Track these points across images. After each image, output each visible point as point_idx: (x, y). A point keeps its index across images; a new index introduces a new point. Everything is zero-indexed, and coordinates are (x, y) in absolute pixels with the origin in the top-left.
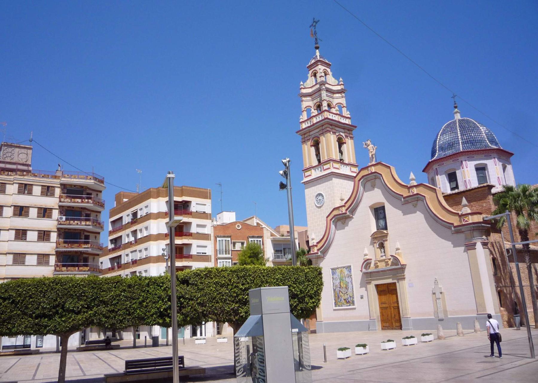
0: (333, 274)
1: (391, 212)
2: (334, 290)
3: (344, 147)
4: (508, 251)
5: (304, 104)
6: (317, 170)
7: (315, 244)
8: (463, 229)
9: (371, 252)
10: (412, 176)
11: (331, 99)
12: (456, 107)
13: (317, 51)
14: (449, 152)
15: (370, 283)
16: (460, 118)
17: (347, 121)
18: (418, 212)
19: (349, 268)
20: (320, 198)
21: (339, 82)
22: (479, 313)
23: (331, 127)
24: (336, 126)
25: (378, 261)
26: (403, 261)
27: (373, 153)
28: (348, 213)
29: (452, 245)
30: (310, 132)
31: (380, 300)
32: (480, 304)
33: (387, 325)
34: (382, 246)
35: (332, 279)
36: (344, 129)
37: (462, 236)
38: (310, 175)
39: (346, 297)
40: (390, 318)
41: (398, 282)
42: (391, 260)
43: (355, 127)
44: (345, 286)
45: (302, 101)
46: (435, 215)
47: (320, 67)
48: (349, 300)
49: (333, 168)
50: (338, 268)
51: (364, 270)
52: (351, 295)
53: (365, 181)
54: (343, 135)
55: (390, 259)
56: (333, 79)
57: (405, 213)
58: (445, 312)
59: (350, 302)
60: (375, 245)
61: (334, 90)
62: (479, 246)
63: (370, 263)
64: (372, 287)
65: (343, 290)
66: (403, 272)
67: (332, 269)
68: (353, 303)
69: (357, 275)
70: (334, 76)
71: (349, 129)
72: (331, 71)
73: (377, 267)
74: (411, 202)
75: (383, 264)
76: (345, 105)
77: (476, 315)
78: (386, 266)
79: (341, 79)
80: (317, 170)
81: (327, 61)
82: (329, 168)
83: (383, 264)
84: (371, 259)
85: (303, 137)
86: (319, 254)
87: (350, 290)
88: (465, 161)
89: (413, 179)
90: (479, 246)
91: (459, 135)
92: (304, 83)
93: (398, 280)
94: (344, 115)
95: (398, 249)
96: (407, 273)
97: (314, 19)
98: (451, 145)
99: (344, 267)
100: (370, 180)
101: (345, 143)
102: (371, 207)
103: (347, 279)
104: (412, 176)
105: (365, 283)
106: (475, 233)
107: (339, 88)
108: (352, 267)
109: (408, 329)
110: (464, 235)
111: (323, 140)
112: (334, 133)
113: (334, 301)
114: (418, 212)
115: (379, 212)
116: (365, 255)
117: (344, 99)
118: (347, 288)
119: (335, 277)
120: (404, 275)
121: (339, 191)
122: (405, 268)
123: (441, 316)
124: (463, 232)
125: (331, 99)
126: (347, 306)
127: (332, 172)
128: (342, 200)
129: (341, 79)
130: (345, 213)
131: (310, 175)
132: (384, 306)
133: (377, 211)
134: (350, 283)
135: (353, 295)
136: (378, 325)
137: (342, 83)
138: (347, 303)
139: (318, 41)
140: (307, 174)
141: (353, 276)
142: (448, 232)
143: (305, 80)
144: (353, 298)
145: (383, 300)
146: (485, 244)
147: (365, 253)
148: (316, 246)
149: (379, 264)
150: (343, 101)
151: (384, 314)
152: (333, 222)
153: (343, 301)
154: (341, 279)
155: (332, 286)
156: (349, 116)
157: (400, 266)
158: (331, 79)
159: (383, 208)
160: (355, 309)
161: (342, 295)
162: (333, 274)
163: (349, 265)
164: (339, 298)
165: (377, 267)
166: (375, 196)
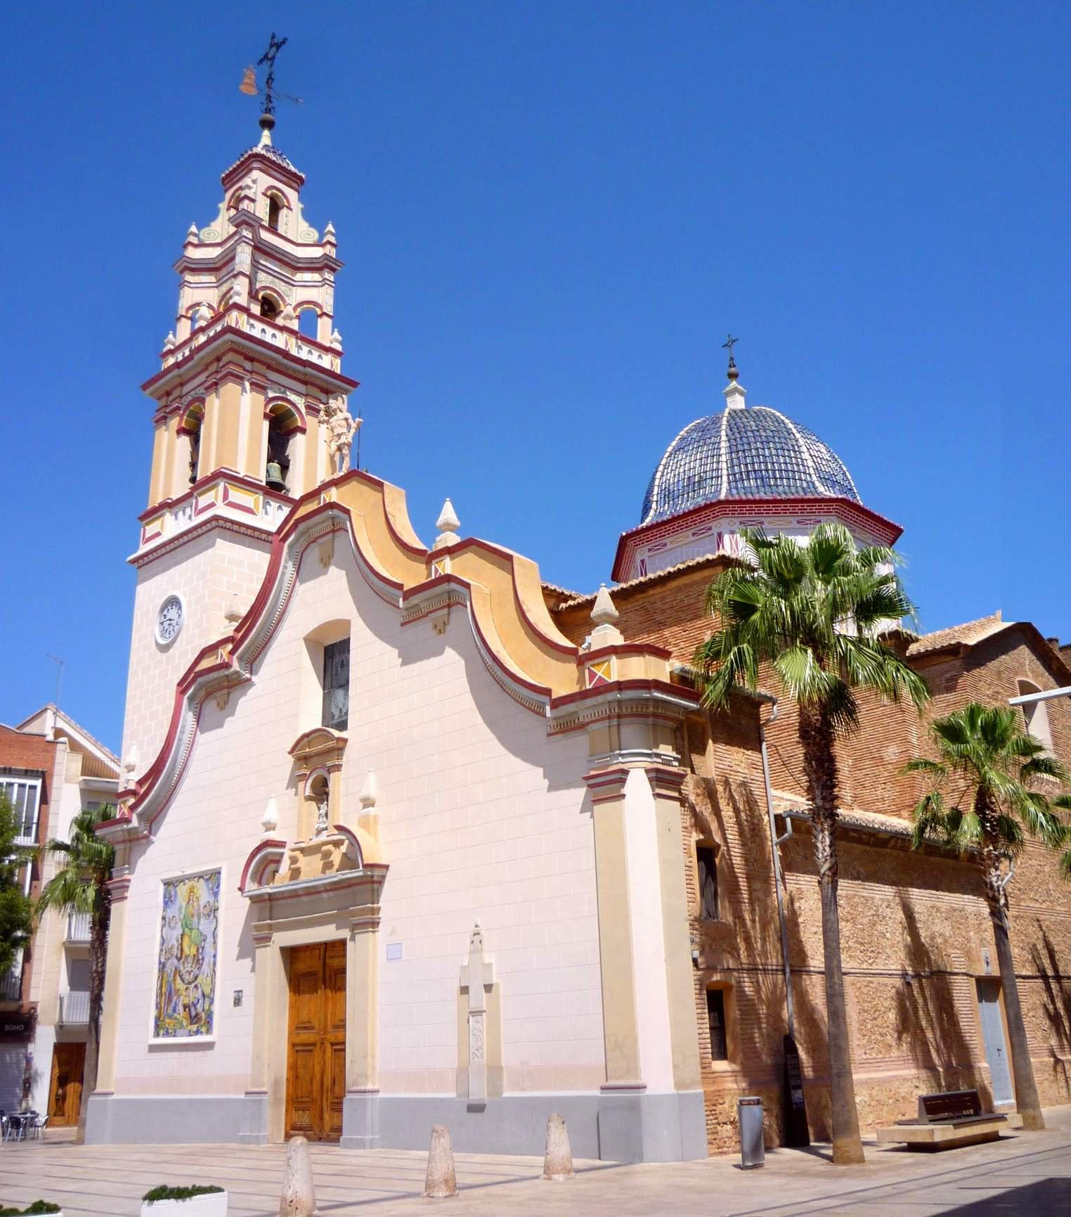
0: (166, 903)
1: (370, 655)
2: (162, 966)
3: (297, 447)
4: (779, 820)
5: (188, 297)
6: (180, 514)
7: (132, 786)
8: (583, 710)
9: (285, 815)
10: (448, 513)
11: (281, 287)
12: (733, 376)
14: (686, 505)
15: (268, 939)
17: (326, 361)
18: (449, 652)
20: (172, 613)
21: (322, 234)
22: (612, 1083)
23: (248, 365)
24: (269, 367)
25: (302, 850)
26: (373, 851)
27: (343, 440)
28: (236, 666)
29: (546, 782)
30: (182, 385)
31: (294, 1008)
32: (620, 1044)
33: (305, 1119)
34: (321, 793)
35: (159, 922)
36: (306, 383)
37: (579, 743)
38: (158, 534)
40: (316, 1095)
41: (353, 939)
42: (343, 848)
43: (354, 384)
44: (193, 951)
45: (182, 284)
46: (495, 659)
47: (256, 174)
49: (215, 502)
50: (181, 880)
51: (251, 887)
52: (207, 991)
53: (303, 543)
54: (300, 402)
55: (337, 844)
56: (304, 225)
57: (408, 658)
58: (495, 1070)
59: (200, 1019)
60: (301, 785)
61: (298, 259)
62: (638, 784)
63: (277, 861)
64: (270, 958)
65: (186, 968)
66: (375, 896)
67: (168, 884)
69: (233, 910)
70: (308, 215)
71: (323, 386)
72: (300, 199)
73: (295, 873)
74: (427, 609)
75: (316, 862)
76: (329, 309)
77: (597, 1093)
78: (323, 872)
79: (330, 228)
80: (180, 514)
81: (292, 168)
82: (212, 505)
83: (316, 862)
84: (281, 844)
85: (163, 402)
86: (135, 822)
87: (206, 968)
88: (732, 533)
89: (449, 527)
90: (638, 784)
91: (723, 451)
92: (199, 229)
93: (356, 927)
94: (319, 340)
95: (368, 803)
96: (389, 902)
98: (695, 484)
99: (200, 876)
100: (314, 532)
101: (303, 431)
102: (310, 641)
104: (448, 513)
105: (254, 940)
106: (630, 731)
107: (317, 252)
109: (360, 1144)
110: (575, 732)
111: (214, 406)
112: (258, 387)
113: (153, 1013)
114: (449, 652)
115: (333, 659)
116: (269, 827)
117: (331, 291)
118: (198, 961)
120: (375, 911)
121: (221, 581)
122: (381, 882)
123: (479, 1093)
124: (582, 726)
125: (281, 287)
127: (216, 518)
128: (231, 618)
129: (330, 228)
130: (226, 666)
131: (158, 534)
132: (306, 1037)
133: (332, 657)
134: (210, 940)
135: (213, 990)
136: (274, 1117)
137: (333, 240)
139: (275, 103)
140: (151, 529)
141: (221, 914)
142: (535, 729)
143: (206, 219)
145: (304, 1016)
146: (663, 781)
147: (265, 818)
149: (303, 862)
150: (325, 297)
151: (301, 1071)
152: (191, 699)
153: (181, 1014)
156: (339, 347)
157: (359, 873)
158: (294, 223)
159: (344, 646)
160: (209, 1046)
162: (168, 901)
164: (170, 1000)
165: (295, 873)
166: (323, 599)
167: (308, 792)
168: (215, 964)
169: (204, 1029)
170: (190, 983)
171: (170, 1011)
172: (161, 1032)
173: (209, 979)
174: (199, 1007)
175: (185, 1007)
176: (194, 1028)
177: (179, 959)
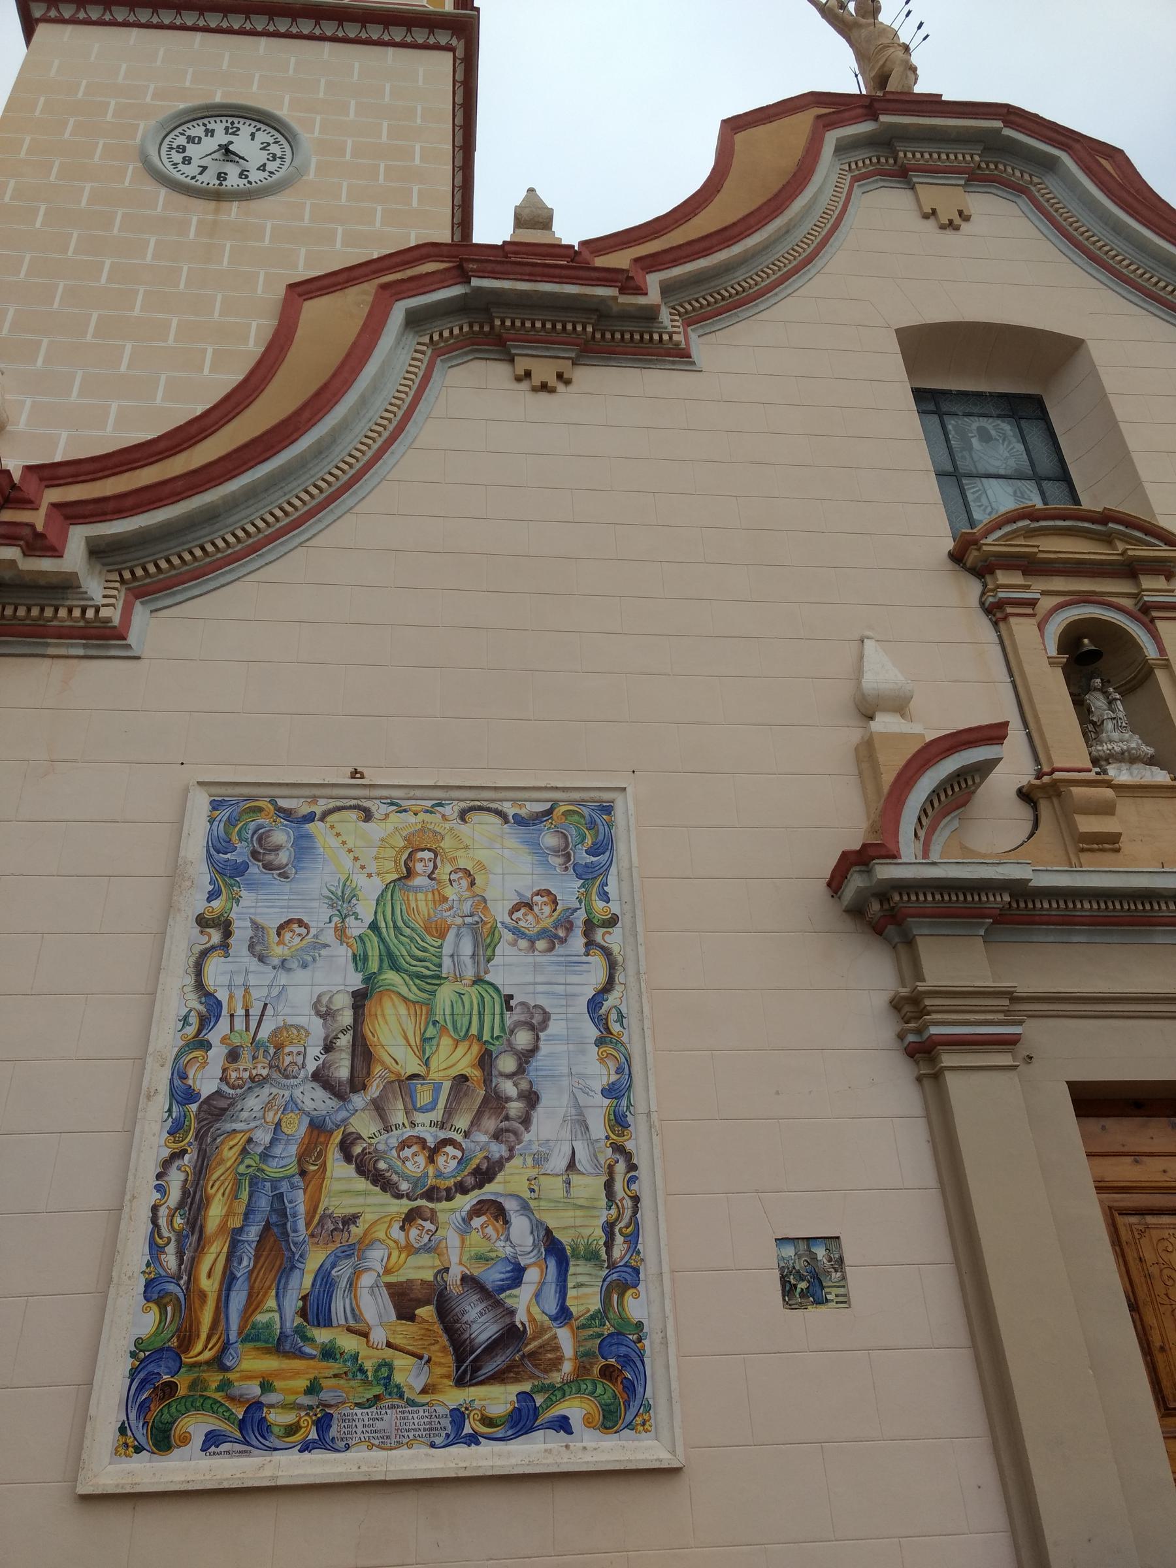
0: (227, 874)
2: (200, 1121)
19: (582, 831)
35: (184, 938)
39: (458, 1245)
48: (524, 1302)
52: (580, 1226)
68: (618, 1376)
103: (513, 969)
118: (497, 1092)
126: (458, 1429)
130: (627, 283)
134: (570, 1028)
135: (625, 1227)
138: (469, 1366)
144: (624, 1279)
154: (389, 961)
155: (167, 1039)
167: (1053, 651)
168: (619, 1122)
169: (574, 1409)
170: (431, 1194)
171: (279, 1312)
172: (196, 1426)
173: (589, 1186)
174: (524, 1302)
175: (404, 1301)
176: (498, 1399)
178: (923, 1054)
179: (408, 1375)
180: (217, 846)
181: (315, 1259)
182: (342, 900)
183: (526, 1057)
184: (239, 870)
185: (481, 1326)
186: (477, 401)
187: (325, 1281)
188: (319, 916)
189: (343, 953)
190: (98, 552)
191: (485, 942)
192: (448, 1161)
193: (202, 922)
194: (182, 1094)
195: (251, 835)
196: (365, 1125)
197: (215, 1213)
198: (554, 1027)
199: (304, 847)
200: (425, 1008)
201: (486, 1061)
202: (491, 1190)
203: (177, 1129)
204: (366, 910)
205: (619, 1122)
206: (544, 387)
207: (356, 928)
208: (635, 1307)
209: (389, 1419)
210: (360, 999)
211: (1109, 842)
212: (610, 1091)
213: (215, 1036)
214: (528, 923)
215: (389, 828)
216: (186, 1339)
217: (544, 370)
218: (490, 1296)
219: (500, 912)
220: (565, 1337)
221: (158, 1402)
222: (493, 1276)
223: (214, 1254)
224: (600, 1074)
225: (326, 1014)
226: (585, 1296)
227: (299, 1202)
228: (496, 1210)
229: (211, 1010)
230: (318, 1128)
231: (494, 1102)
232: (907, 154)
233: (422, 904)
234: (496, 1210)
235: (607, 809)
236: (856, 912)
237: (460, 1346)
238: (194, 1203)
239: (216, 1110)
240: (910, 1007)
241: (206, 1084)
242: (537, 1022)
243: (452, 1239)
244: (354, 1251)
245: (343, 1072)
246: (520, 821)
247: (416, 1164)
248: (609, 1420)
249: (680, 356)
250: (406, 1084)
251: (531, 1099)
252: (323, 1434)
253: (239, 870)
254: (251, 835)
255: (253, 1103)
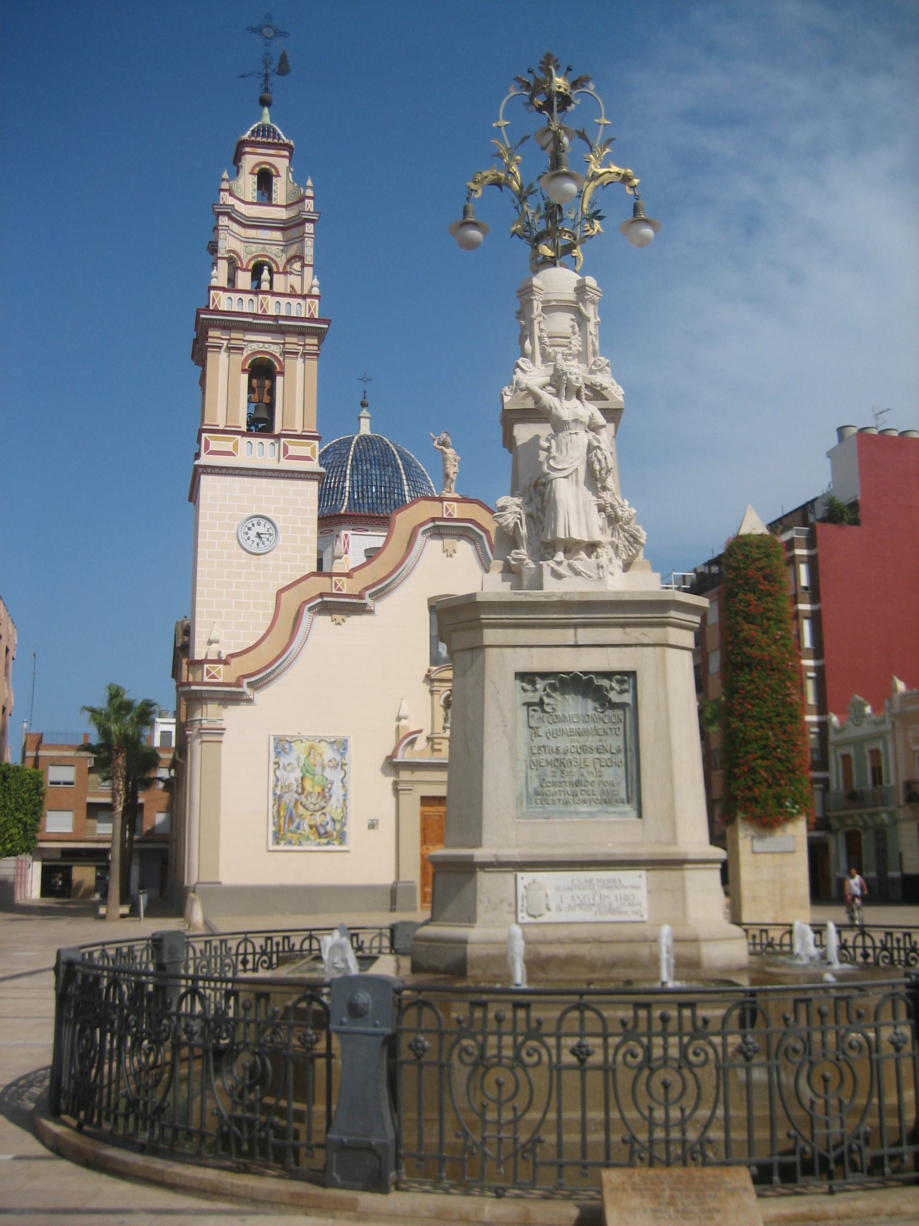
0: (278, 754)
2: (278, 799)
13: (266, 110)
16: (369, 433)
19: (341, 745)
35: (272, 767)
39: (318, 819)
44: (318, 789)
48: (329, 828)
52: (338, 817)
59: (331, 834)
65: (310, 801)
68: (342, 837)
82: (308, 459)
97: (268, 17)
102: (430, 600)
103: (328, 773)
108: (351, 745)
113: (272, 828)
118: (325, 795)
119: (283, 760)
126: (319, 844)
135: (345, 817)
138: (320, 836)
141: (352, 769)
144: (344, 825)
148: (226, 663)
154: (307, 772)
155: (271, 785)
161: (306, 813)
163: (342, 734)
164: (291, 820)
167: (442, 703)
168: (345, 800)
169: (336, 842)
171: (293, 827)
172: (283, 842)
173: (339, 810)
175: (311, 827)
176: (325, 841)
177: (300, 794)
178: (396, 792)
179: (312, 837)
180: (276, 748)
181: (297, 821)
182: (298, 759)
183: (330, 789)
184: (279, 753)
185: (322, 831)
186: (323, 621)
187: (299, 824)
188: (295, 763)
189: (299, 770)
190: (249, 683)
191: (323, 768)
192: (317, 806)
193: (275, 763)
194: (275, 794)
195: (281, 746)
196: (304, 800)
197: (282, 813)
198: (335, 784)
199: (291, 749)
200: (313, 780)
201: (323, 790)
202: (324, 811)
203: (275, 800)
204: (302, 761)
205: (345, 800)
206: (339, 624)
207: (301, 765)
208: (345, 829)
209: (309, 842)
210: (302, 778)
211: (439, 750)
212: (344, 795)
213: (279, 784)
214: (331, 764)
215: (306, 744)
216: (280, 831)
217: (339, 618)
218: (324, 827)
219: (326, 762)
220: (335, 833)
221: (277, 839)
222: (324, 824)
223: (282, 820)
224: (342, 792)
225: (297, 781)
226: (338, 827)
227: (294, 812)
228: (324, 814)
229: (278, 780)
230: (297, 801)
231: (324, 797)
232: (442, 531)
233: (312, 760)
234: (324, 814)
235: (346, 740)
236: (390, 763)
237: (319, 834)
238: (278, 811)
239: (280, 797)
240: (396, 783)
241: (278, 793)
242: (332, 783)
243: (318, 818)
244: (304, 819)
245: (300, 791)
246: (330, 743)
247: (312, 807)
248: (341, 844)
249: (371, 612)
250: (310, 793)
251: (330, 796)
252: (300, 844)
253: (279, 753)
254: (281, 746)
255: (286, 796)
